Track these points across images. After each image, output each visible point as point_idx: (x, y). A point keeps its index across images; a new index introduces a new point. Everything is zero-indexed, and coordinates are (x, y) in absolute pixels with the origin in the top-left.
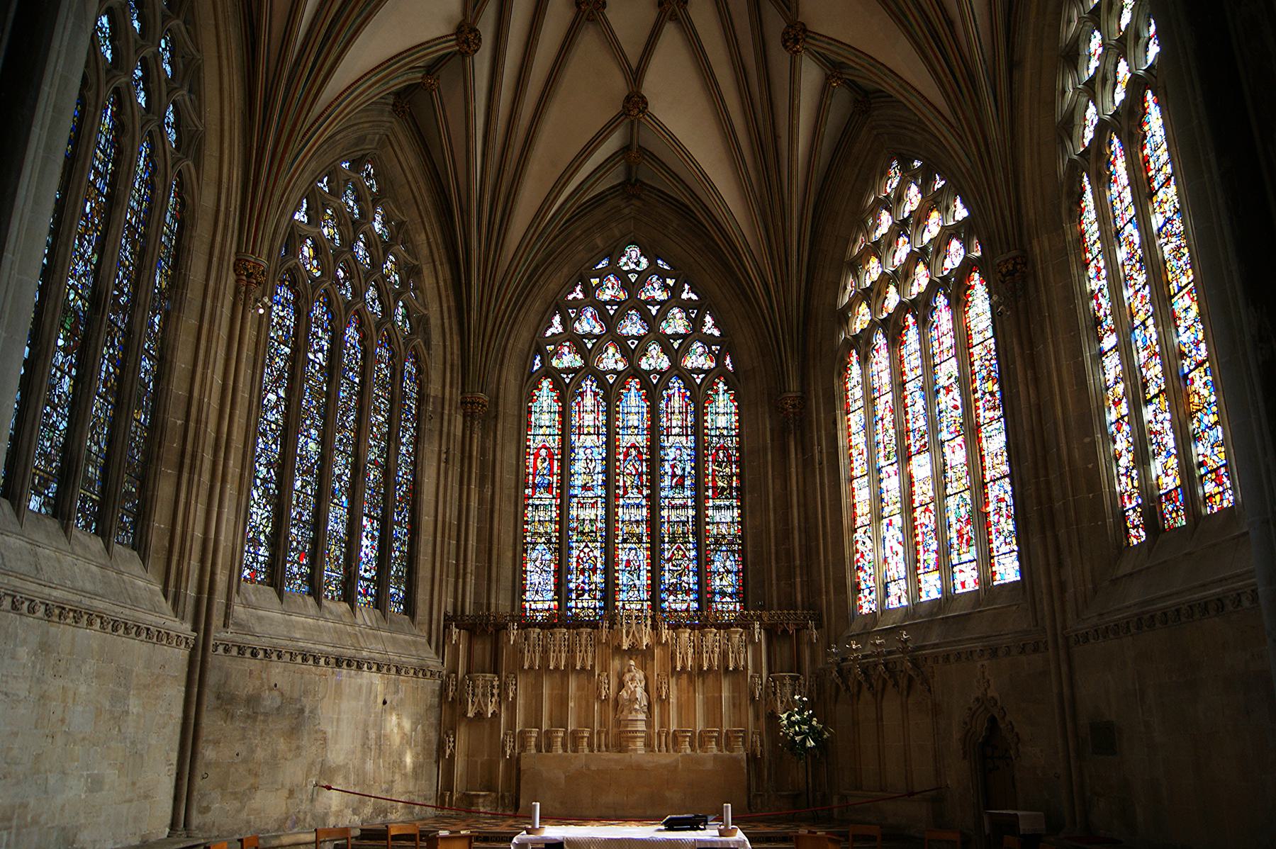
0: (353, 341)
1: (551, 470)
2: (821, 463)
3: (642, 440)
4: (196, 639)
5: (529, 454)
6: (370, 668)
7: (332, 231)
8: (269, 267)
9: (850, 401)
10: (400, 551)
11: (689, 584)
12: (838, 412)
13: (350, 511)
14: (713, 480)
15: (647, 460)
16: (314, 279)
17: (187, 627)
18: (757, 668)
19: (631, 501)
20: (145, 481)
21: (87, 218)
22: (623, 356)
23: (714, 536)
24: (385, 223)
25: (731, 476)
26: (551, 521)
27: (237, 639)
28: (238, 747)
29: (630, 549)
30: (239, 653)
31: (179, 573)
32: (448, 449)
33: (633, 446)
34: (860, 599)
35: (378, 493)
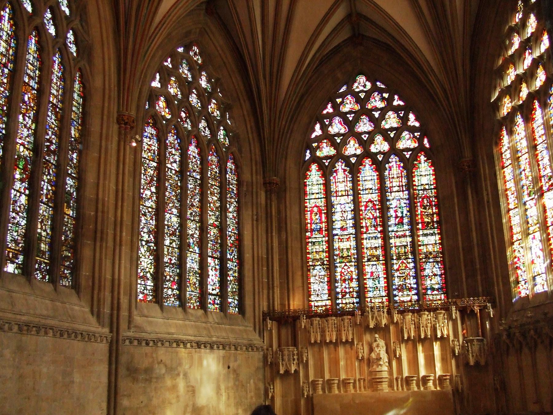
0: (194, 154)
1: (321, 220)
2: (488, 202)
3: (375, 197)
4: (112, 337)
5: (307, 211)
6: (218, 348)
7: (176, 90)
8: (137, 117)
9: (504, 160)
10: (233, 276)
11: (410, 284)
12: (497, 168)
13: (201, 255)
14: (422, 218)
15: (379, 209)
16: (167, 120)
17: (106, 330)
18: (456, 335)
19: (372, 235)
20: (75, 247)
21: (27, 104)
22: (360, 145)
23: (425, 254)
24: (209, 81)
25: (433, 214)
26: (323, 251)
27: (137, 336)
28: (141, 398)
29: (373, 265)
30: (139, 344)
31: (99, 300)
32: (257, 212)
33: (370, 201)
34: (519, 288)
35: (217, 243)
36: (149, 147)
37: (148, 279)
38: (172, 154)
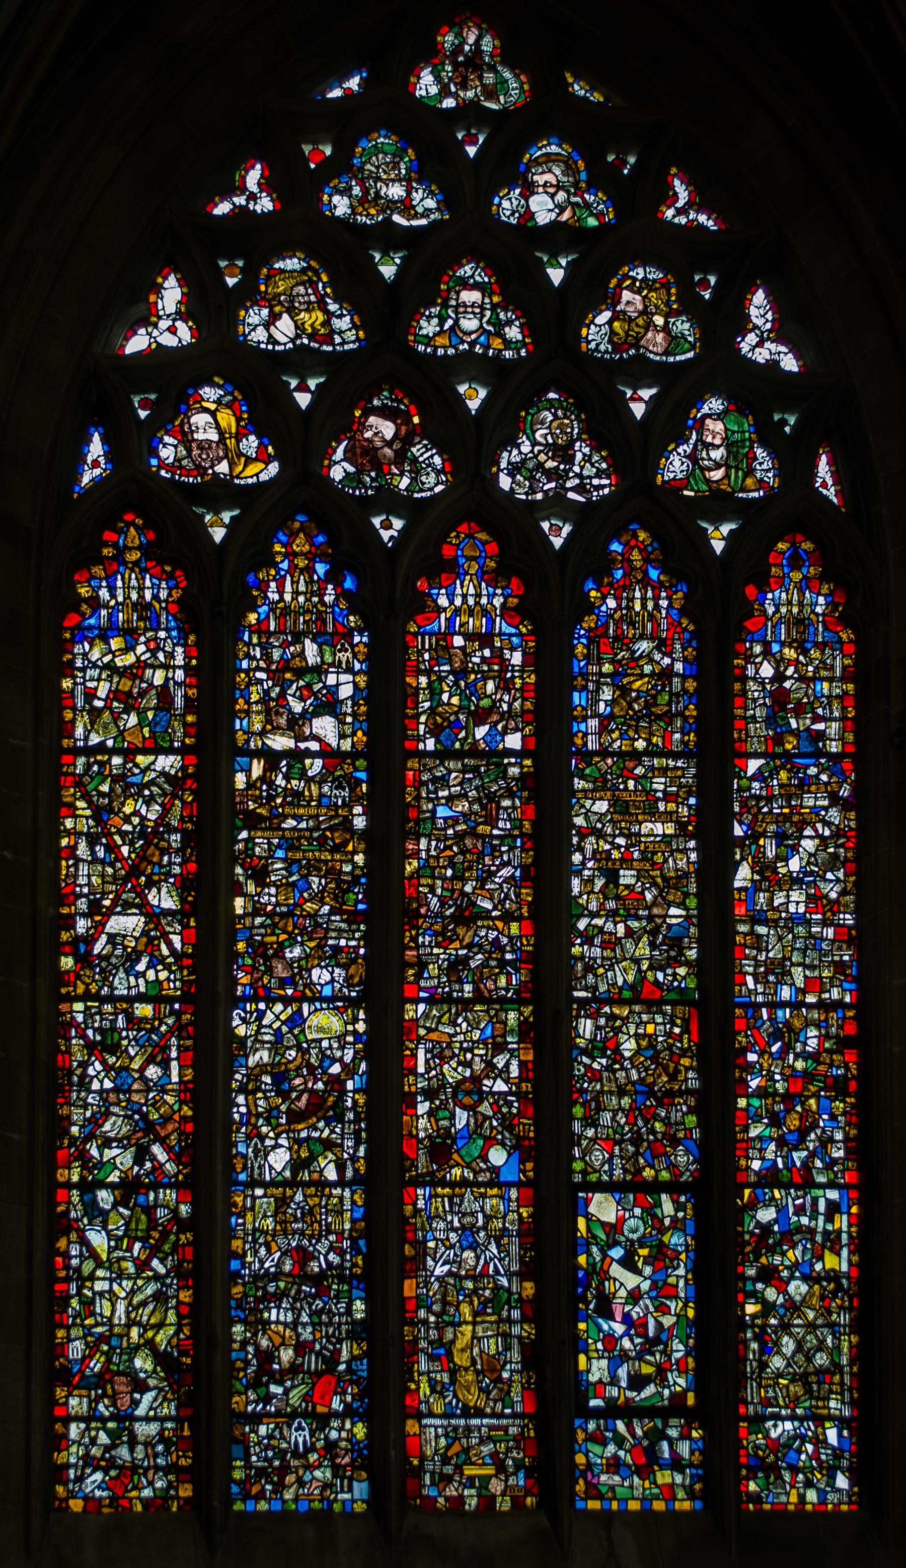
36: (125, 685)
37: (142, 1387)
38: (300, 673)
